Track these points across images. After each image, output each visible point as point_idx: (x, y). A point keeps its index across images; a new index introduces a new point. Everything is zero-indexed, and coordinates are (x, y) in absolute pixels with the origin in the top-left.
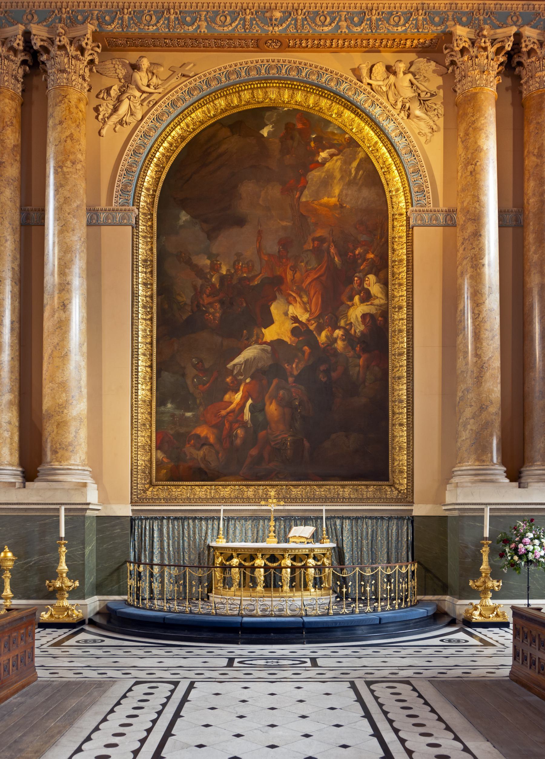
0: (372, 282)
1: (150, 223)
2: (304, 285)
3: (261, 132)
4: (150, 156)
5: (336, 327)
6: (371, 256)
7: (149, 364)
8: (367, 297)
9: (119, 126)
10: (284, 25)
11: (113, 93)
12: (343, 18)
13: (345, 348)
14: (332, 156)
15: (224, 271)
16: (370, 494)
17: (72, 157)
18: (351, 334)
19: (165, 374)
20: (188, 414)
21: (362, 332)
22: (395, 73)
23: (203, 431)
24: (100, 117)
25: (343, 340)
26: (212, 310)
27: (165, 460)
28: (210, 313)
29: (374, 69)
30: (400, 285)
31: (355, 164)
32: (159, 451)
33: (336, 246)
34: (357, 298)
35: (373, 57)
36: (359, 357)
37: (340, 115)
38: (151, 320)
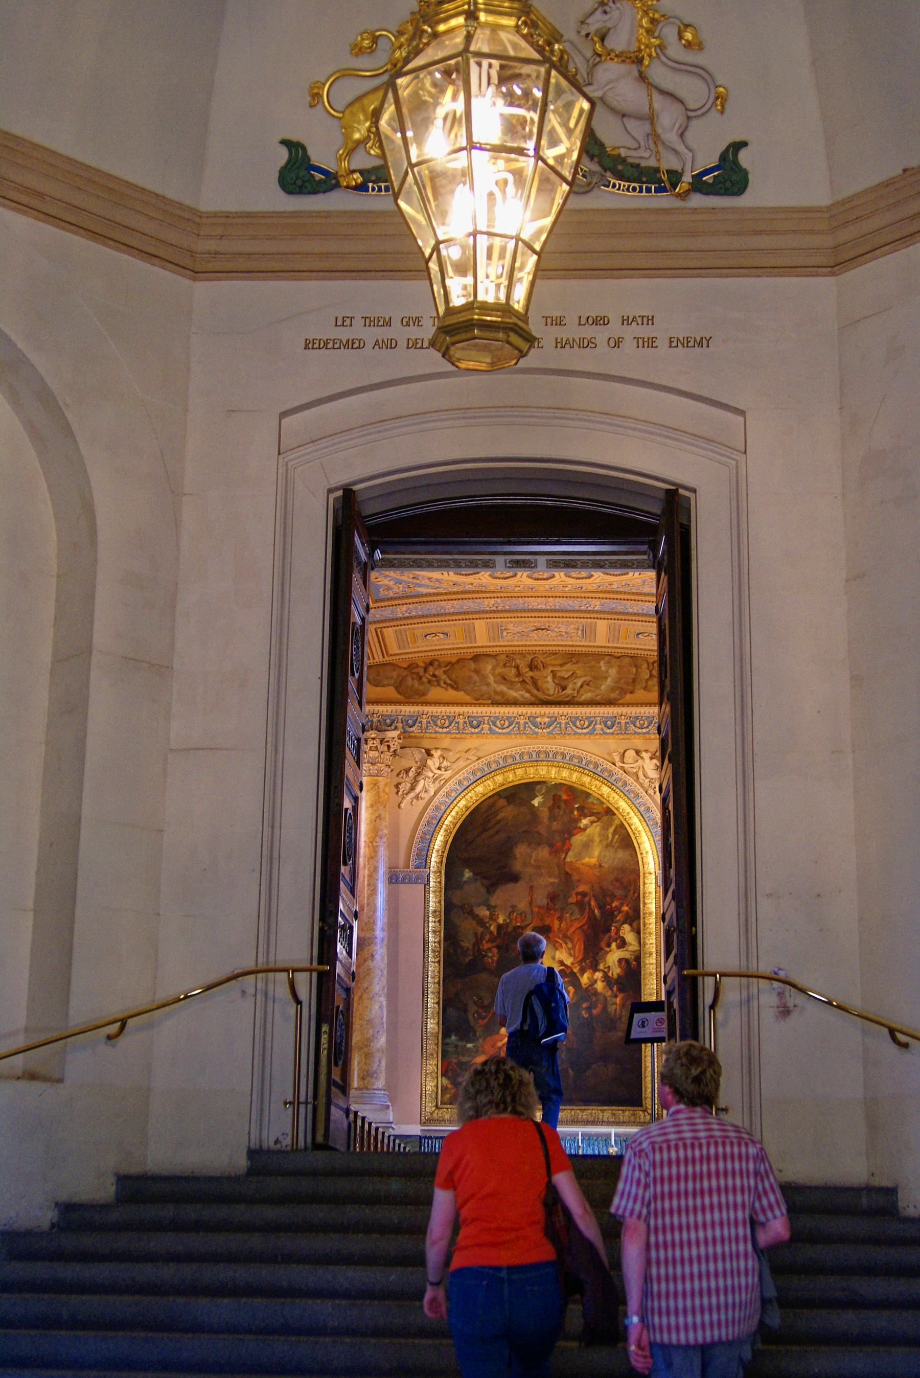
0: (627, 932)
1: (438, 880)
2: (569, 933)
3: (533, 802)
4: (440, 824)
5: (595, 969)
6: (625, 908)
7: (436, 1000)
8: (623, 944)
9: (415, 801)
10: (551, 728)
11: (411, 774)
12: (598, 722)
13: (604, 988)
14: (592, 822)
15: (501, 921)
16: (626, 1119)
17: (380, 833)
18: (609, 977)
19: (450, 1010)
20: (470, 1045)
21: (618, 975)
22: (642, 758)
24: (400, 793)
25: (603, 981)
26: (490, 954)
27: (449, 1086)
28: (489, 957)
29: (627, 752)
30: (650, 933)
31: (611, 830)
32: (444, 1078)
33: (596, 900)
34: (614, 945)
36: (616, 996)
37: (599, 789)
38: (439, 962)
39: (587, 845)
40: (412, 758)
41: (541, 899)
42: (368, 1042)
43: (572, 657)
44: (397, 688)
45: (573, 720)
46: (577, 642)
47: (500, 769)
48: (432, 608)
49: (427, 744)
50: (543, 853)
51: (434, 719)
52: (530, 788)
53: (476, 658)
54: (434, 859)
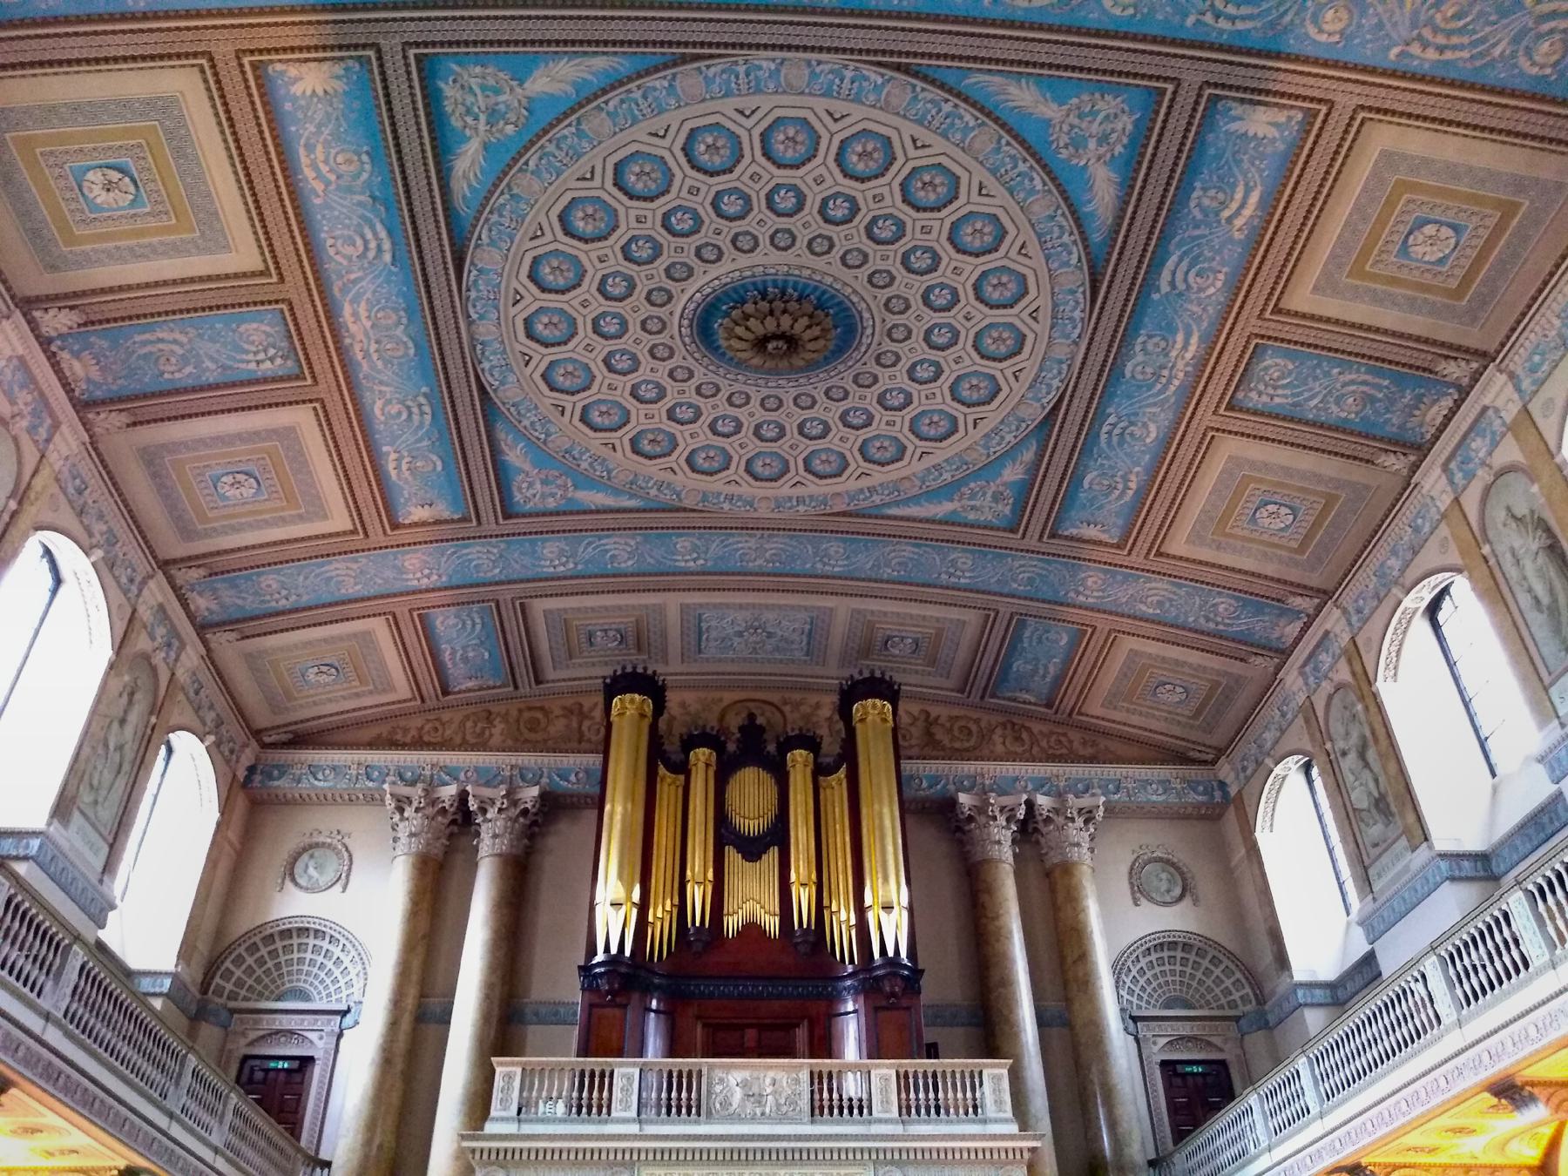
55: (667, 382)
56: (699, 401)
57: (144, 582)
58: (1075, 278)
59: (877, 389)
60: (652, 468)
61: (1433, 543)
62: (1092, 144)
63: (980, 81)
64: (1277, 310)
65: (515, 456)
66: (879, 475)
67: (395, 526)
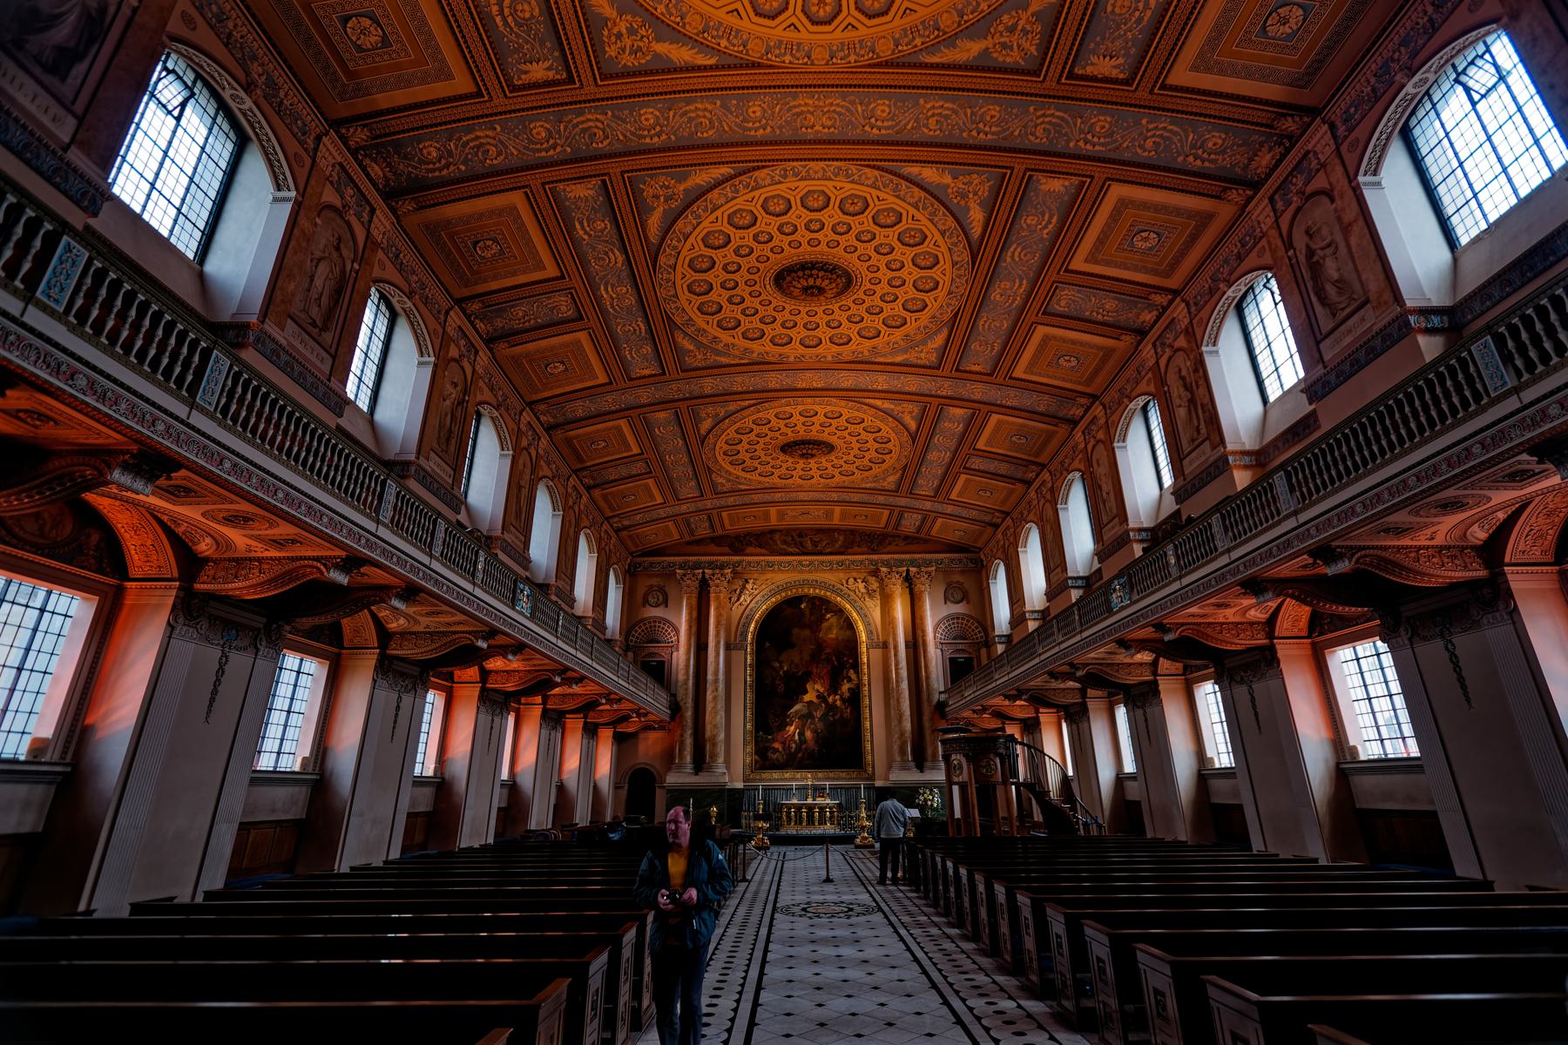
8: (850, 680)
23: (776, 745)
35: (848, 575)
39: (830, 628)
40: (738, 584)
41: (806, 657)
42: (714, 737)
43: (819, 531)
44: (731, 547)
45: (822, 563)
46: (823, 522)
47: (784, 589)
48: (747, 499)
49: (746, 576)
50: (807, 632)
51: (749, 563)
52: (797, 600)
53: (772, 532)
54: (750, 636)
55: (759, 307)
56: (775, 314)
57: (521, 413)
58: (966, 257)
59: (865, 306)
60: (754, 345)
61: (1144, 382)
62: (971, 196)
63: (912, 170)
64: (1067, 270)
65: (688, 345)
66: (869, 343)
67: (631, 379)
